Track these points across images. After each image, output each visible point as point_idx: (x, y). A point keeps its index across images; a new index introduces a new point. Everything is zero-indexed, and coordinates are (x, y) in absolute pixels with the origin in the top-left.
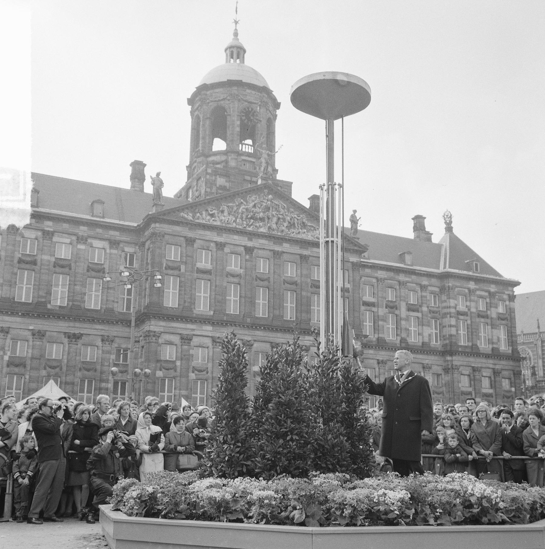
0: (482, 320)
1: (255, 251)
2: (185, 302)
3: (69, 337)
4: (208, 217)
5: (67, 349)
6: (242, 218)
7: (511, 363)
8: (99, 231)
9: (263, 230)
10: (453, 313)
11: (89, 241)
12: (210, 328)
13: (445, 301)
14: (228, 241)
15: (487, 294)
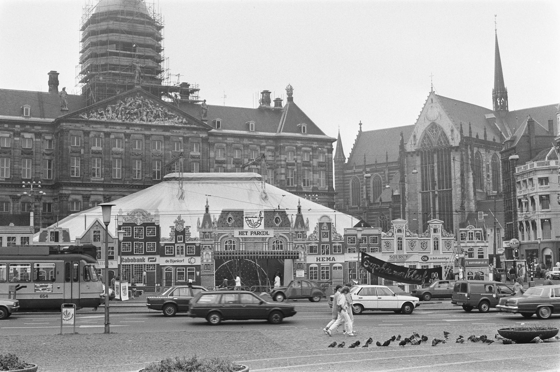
0: (306, 168)
1: (132, 135)
2: (84, 173)
3: (13, 198)
4: (98, 116)
5: (12, 205)
6: (121, 114)
7: (327, 197)
8: (28, 127)
9: (137, 121)
10: (284, 165)
11: (22, 134)
12: (102, 189)
13: (278, 156)
14: (113, 130)
15: (310, 149)
